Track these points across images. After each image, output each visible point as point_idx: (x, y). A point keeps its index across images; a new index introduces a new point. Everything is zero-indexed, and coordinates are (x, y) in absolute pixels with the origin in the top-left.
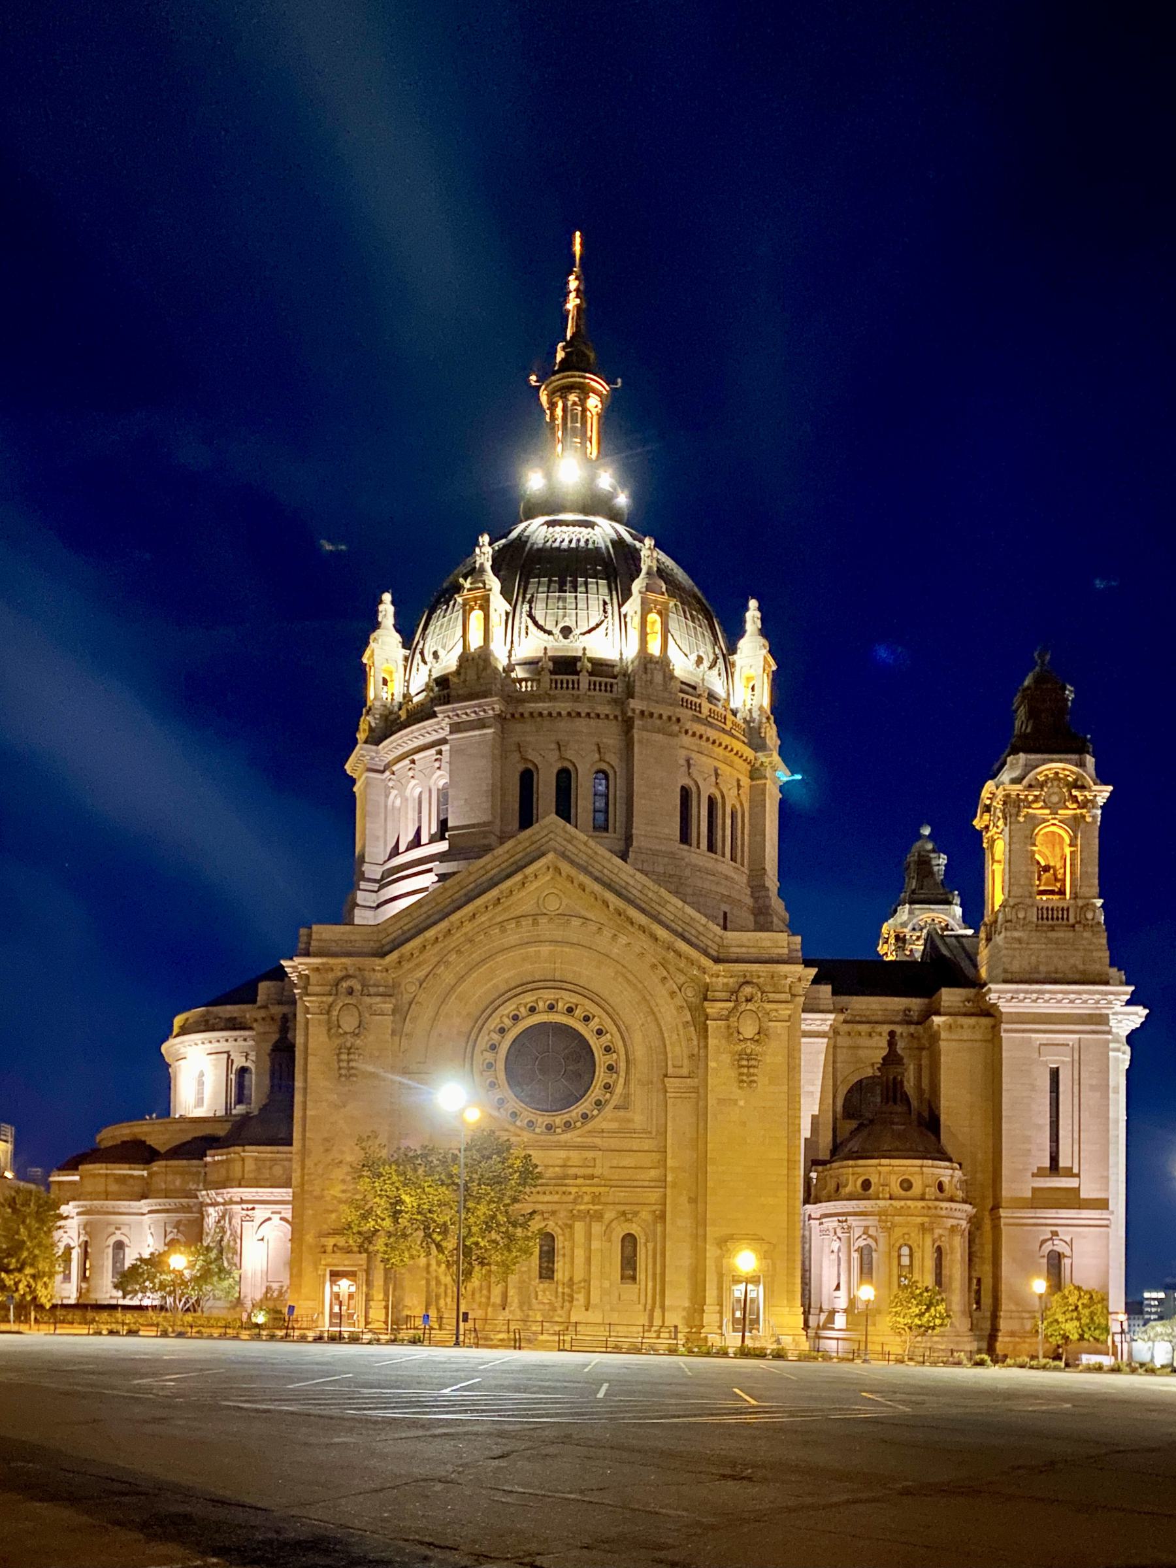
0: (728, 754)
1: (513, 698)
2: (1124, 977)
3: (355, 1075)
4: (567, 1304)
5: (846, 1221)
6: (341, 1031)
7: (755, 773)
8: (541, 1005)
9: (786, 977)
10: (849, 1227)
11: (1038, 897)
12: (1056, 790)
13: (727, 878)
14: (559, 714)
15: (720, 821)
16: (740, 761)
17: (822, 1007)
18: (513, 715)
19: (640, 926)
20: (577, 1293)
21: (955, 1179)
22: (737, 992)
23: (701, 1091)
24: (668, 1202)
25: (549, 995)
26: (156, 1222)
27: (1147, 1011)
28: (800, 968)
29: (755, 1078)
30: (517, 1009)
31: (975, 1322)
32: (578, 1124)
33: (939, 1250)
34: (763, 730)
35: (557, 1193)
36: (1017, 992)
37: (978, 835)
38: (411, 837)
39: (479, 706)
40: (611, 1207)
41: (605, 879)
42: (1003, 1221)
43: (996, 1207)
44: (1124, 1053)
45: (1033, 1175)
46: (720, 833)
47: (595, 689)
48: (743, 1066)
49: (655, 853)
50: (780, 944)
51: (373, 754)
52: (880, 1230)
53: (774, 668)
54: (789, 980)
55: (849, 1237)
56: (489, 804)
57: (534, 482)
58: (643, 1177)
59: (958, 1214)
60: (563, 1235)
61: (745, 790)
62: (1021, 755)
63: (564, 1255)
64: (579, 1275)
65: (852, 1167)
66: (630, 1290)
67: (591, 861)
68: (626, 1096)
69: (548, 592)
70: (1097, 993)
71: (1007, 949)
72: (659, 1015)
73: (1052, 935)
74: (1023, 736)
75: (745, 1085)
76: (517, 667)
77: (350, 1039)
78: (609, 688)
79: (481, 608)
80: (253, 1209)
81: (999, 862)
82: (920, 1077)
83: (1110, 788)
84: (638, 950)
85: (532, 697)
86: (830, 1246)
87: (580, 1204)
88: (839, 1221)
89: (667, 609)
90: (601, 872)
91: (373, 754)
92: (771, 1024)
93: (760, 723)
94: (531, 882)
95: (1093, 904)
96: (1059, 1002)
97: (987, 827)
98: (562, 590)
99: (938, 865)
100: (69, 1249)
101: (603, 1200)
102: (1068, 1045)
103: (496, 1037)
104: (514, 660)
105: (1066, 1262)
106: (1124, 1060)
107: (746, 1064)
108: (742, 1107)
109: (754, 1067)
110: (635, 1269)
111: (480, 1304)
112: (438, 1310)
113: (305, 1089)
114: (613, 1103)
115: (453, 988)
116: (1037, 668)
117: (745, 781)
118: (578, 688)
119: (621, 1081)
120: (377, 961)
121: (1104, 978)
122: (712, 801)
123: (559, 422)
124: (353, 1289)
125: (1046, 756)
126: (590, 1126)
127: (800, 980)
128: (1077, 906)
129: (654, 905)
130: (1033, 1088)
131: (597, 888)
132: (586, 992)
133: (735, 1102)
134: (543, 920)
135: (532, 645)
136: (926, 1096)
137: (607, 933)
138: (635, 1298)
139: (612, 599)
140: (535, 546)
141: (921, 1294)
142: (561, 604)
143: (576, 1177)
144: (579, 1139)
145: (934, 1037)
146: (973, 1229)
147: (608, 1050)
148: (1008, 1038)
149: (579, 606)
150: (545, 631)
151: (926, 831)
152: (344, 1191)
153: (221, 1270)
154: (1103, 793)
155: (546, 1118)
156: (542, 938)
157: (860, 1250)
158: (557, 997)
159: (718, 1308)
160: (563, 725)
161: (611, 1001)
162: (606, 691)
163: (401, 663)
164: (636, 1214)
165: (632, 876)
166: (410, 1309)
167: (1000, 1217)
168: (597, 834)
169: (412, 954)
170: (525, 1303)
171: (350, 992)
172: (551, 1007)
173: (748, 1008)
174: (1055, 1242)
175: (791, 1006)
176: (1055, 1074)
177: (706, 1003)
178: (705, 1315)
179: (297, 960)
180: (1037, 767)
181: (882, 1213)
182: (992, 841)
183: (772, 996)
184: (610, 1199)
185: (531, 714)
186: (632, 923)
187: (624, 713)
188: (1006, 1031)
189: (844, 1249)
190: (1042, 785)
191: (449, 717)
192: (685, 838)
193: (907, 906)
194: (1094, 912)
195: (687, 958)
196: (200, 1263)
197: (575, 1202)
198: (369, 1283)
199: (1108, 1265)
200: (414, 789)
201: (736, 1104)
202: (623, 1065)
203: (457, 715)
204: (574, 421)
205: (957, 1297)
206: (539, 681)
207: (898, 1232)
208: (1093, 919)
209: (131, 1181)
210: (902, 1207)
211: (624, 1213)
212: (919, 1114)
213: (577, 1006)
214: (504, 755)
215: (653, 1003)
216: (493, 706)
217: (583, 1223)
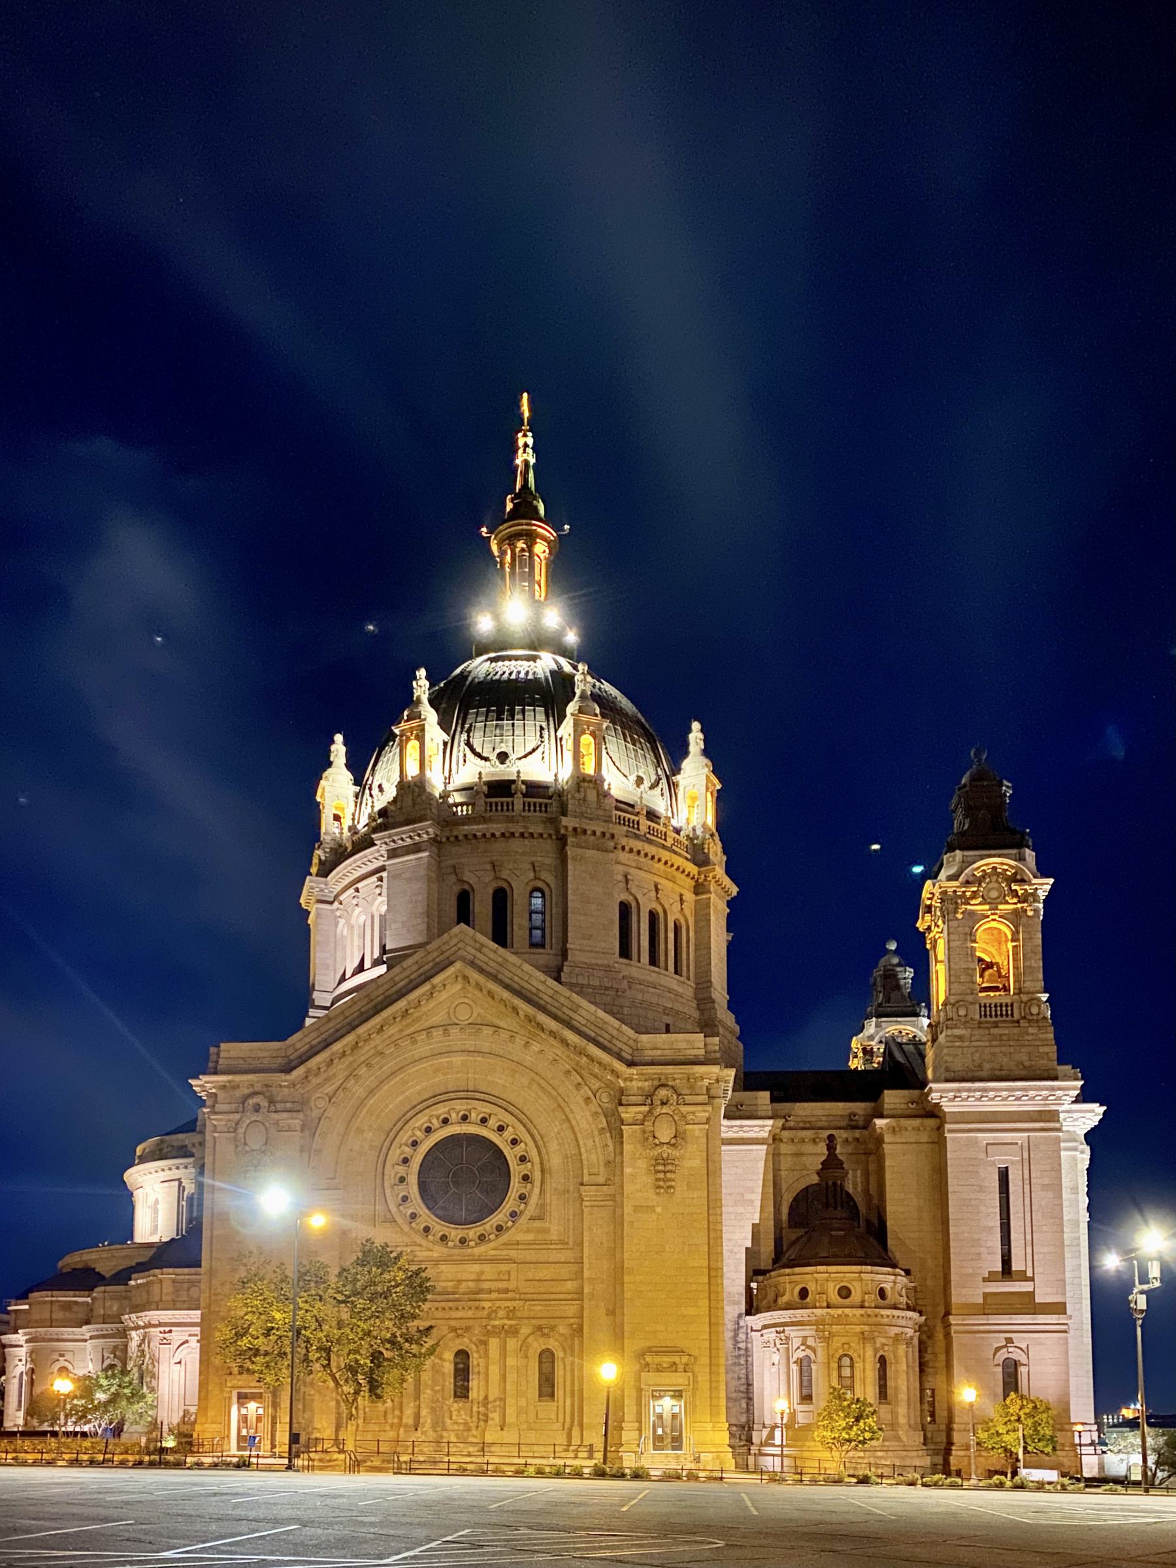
0: (669, 870)
2: (1080, 1075)
5: (783, 1331)
6: (247, 1148)
11: (981, 995)
13: (670, 991)
14: (493, 835)
15: (662, 936)
16: (683, 876)
17: (759, 1113)
19: (551, 1032)
21: (899, 1286)
22: (650, 1096)
23: (618, 1198)
24: (585, 1315)
25: (461, 1107)
29: (673, 1183)
31: (929, 1435)
32: (492, 1237)
33: (882, 1361)
34: (706, 846)
35: (470, 1308)
36: (959, 1090)
37: (922, 936)
38: (356, 963)
39: (413, 831)
40: (526, 1321)
41: (516, 986)
42: (953, 1328)
43: (948, 1313)
44: (1082, 1152)
45: (984, 1280)
46: (662, 946)
47: (529, 810)
48: (659, 1172)
49: (592, 967)
51: (323, 886)
52: (818, 1340)
53: (719, 787)
54: (706, 1082)
55: (788, 1348)
56: (425, 926)
58: (558, 1290)
60: (478, 1352)
66: (548, 1409)
67: (502, 969)
68: (542, 1206)
69: (486, 721)
70: (1046, 1089)
71: (947, 1047)
72: (574, 1122)
73: (994, 1031)
74: (962, 834)
75: (662, 1191)
76: (455, 793)
78: (543, 809)
81: (941, 962)
82: (868, 1183)
83: (1051, 881)
85: (467, 820)
88: (777, 1332)
89: (600, 730)
90: (511, 979)
91: (323, 886)
92: (688, 1127)
94: (440, 991)
95: (1039, 999)
96: (1005, 1099)
97: (929, 928)
99: (905, 978)
102: (1017, 1144)
103: (408, 1150)
104: (450, 787)
105: (1023, 1370)
106: (1083, 1159)
107: (663, 1169)
108: (659, 1214)
109: (671, 1171)
110: (553, 1386)
115: (362, 1103)
117: (689, 897)
118: (513, 810)
119: (537, 1191)
120: (283, 1076)
122: (653, 916)
126: (505, 1237)
128: (1022, 1002)
129: (565, 1010)
130: (981, 1189)
131: (506, 994)
132: (499, 1102)
133: (652, 1209)
134: (454, 1031)
135: (469, 772)
136: (875, 1201)
138: (553, 1417)
139: (548, 725)
140: (476, 680)
142: (498, 732)
143: (490, 1291)
144: (493, 1252)
145: (879, 1140)
146: (924, 1337)
147: (523, 1159)
148: (953, 1139)
149: (516, 733)
151: (892, 946)
155: (459, 1231)
156: (455, 1049)
157: (800, 1362)
159: (637, 1425)
160: (499, 846)
161: (525, 1109)
162: (541, 811)
163: (352, 799)
164: (553, 1328)
165: (544, 983)
168: (532, 950)
169: (319, 1069)
172: (465, 1118)
173: (664, 1111)
174: (1011, 1350)
176: (1004, 1175)
177: (621, 1109)
181: (819, 1323)
182: (935, 942)
183: (688, 1099)
184: (526, 1314)
185: (466, 836)
186: (543, 1030)
187: (557, 831)
188: (950, 1131)
189: (784, 1361)
192: (625, 952)
193: (874, 1019)
195: (600, 1063)
197: (489, 1318)
199: (1068, 1373)
200: (359, 917)
202: (537, 1175)
203: (394, 841)
205: (904, 1411)
206: (473, 805)
207: (837, 1342)
211: (540, 1328)
212: (868, 1221)
213: (490, 1115)
216: (427, 830)
217: (498, 1340)
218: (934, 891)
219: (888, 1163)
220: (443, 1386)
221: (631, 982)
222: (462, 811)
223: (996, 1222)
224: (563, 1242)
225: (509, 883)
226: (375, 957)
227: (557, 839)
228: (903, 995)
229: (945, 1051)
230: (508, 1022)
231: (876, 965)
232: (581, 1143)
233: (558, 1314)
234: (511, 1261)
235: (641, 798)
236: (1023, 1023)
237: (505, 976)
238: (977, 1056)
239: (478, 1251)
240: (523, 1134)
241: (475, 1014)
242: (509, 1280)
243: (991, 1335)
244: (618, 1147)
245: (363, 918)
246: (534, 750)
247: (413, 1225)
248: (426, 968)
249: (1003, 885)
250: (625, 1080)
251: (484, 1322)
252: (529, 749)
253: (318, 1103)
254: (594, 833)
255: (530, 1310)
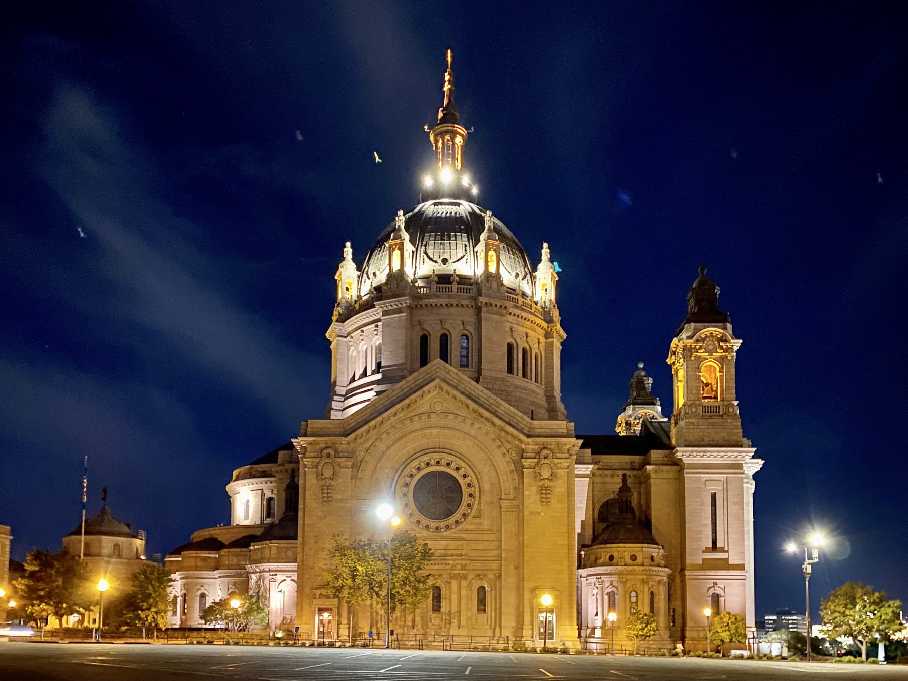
0: (533, 325)
1: (416, 296)
2: (751, 443)
3: (331, 501)
4: (447, 625)
5: (601, 578)
7: (548, 335)
8: (433, 462)
9: (566, 445)
10: (603, 581)
11: (703, 400)
12: (711, 342)
13: (533, 392)
14: (442, 305)
16: (540, 329)
17: (586, 461)
18: (416, 306)
19: (486, 418)
20: (454, 619)
21: (661, 554)
22: (539, 453)
23: (520, 507)
24: (503, 567)
25: (437, 456)
26: (223, 582)
27: (764, 461)
28: (573, 440)
30: (420, 464)
31: (672, 633)
32: (453, 526)
33: (652, 594)
34: (551, 312)
35: (442, 564)
36: (692, 452)
37: (670, 367)
38: (361, 371)
39: (398, 301)
40: (471, 571)
41: (467, 393)
42: (687, 577)
43: (683, 569)
44: (751, 484)
45: (703, 552)
47: (460, 292)
48: (543, 494)
49: (496, 379)
50: (563, 427)
53: (557, 279)
54: (568, 446)
55: (603, 587)
56: (404, 354)
57: (427, 181)
59: (662, 574)
60: (446, 587)
61: (542, 345)
62: (692, 324)
63: (446, 599)
64: (454, 609)
65: (603, 548)
66: (482, 617)
68: (479, 510)
69: (435, 240)
71: (686, 428)
72: (497, 467)
73: (710, 420)
74: (693, 314)
76: (418, 280)
77: (328, 482)
78: (468, 291)
79: (399, 249)
80: (276, 574)
81: (681, 381)
82: (640, 498)
83: (741, 341)
84: (485, 431)
85: (427, 296)
86: (592, 592)
87: (455, 570)
89: (499, 248)
91: (341, 328)
93: (550, 308)
95: (733, 404)
97: (674, 363)
98: (442, 239)
99: (648, 384)
100: (175, 597)
101: (467, 567)
103: (408, 479)
105: (722, 599)
106: (751, 488)
107: (545, 492)
110: (485, 606)
111: (400, 625)
112: (377, 629)
113: (304, 509)
114: (472, 514)
116: (700, 277)
117: (543, 340)
119: (477, 502)
120: (343, 438)
121: (739, 444)
122: (524, 350)
123: (440, 150)
124: (330, 618)
125: (707, 324)
126: (460, 527)
127: (573, 446)
131: (462, 397)
133: (539, 513)
134: (433, 415)
135: (426, 268)
136: (644, 509)
137: (469, 422)
138: (485, 622)
139: (469, 244)
141: (642, 618)
142: (442, 247)
143: (452, 555)
144: (454, 535)
145: (648, 477)
146: (670, 581)
148: (688, 477)
149: (452, 248)
150: (434, 261)
151: (641, 366)
152: (325, 565)
153: (259, 608)
154: (737, 344)
155: (435, 523)
156: (434, 426)
157: (609, 594)
158: (441, 457)
159: (531, 626)
160: (444, 311)
161: (470, 459)
163: (356, 279)
164: (485, 575)
165: (482, 392)
166: (362, 628)
167: (685, 575)
168: (463, 369)
169: (362, 435)
170: (425, 625)
171: (329, 456)
172: (438, 463)
173: (545, 462)
174: (716, 588)
175: (569, 460)
176: (714, 496)
177: (523, 460)
178: (524, 630)
179: (300, 439)
180: (701, 330)
181: (620, 574)
183: (558, 455)
184: (471, 567)
185: (426, 305)
186: (482, 417)
187: (476, 304)
188: (687, 473)
189: (600, 594)
190: (703, 340)
191: (382, 307)
192: (510, 370)
193: (631, 406)
194: (734, 408)
195: (512, 435)
196: (247, 605)
198: (339, 615)
200: (363, 346)
201: (540, 515)
202: (477, 494)
203: (386, 306)
204: (448, 150)
205: (662, 619)
206: (430, 288)
207: (629, 584)
208: (733, 412)
209: (210, 560)
210: (631, 570)
211: (479, 575)
212: (640, 520)
213: (452, 462)
214: (412, 326)
215: (493, 459)
216: (406, 301)
218: (679, 344)
219: (653, 489)
220: (427, 605)
221: (516, 387)
222: (424, 291)
223: (709, 522)
224: (490, 530)
225: (449, 331)
226: (373, 369)
227: (476, 308)
228: (647, 394)
229: (684, 430)
230: (463, 412)
231: (632, 377)
232: (500, 477)
233: (488, 568)
234: (463, 539)
235: (519, 286)
236: (725, 417)
237: (461, 387)
238: (701, 434)
239: (445, 534)
240: (470, 472)
241: (444, 407)
242: (462, 549)
243: (707, 581)
244: (520, 480)
245: (365, 346)
246: (462, 258)
247: (411, 519)
248: (417, 383)
249: (716, 342)
250: (525, 445)
251: (449, 571)
252: (459, 257)
253: (361, 454)
254: (496, 305)
255: (474, 566)
